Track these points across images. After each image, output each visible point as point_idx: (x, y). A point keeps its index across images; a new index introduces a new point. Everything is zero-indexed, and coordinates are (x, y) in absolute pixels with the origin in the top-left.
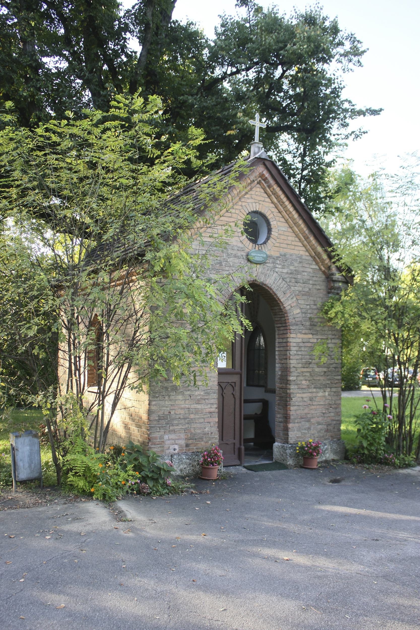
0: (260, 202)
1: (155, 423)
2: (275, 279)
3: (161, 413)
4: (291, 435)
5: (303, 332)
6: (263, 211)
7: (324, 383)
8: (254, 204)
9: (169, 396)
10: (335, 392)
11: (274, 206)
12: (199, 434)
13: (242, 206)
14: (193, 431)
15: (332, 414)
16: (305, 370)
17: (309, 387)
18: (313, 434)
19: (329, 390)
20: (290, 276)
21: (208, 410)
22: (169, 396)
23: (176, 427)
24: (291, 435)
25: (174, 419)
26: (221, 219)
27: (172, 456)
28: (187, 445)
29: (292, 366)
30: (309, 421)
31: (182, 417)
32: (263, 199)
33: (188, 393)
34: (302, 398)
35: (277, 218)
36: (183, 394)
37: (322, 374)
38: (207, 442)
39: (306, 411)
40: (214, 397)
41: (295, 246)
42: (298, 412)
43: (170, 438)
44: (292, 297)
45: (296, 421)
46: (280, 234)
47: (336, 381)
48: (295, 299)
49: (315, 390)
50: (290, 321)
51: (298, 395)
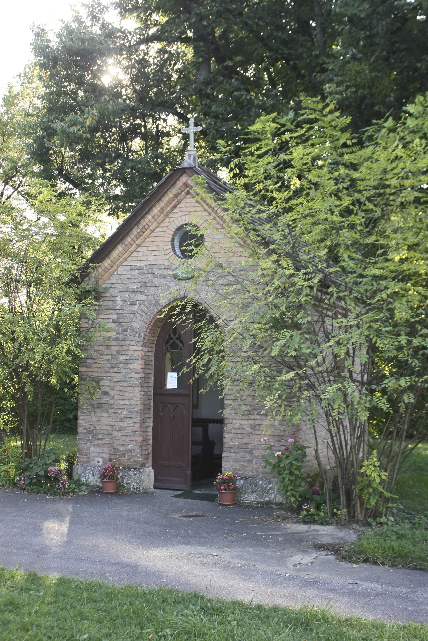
0: (191, 213)
3: (87, 427)
4: (226, 465)
8: (184, 217)
9: (95, 412)
12: (122, 450)
13: (170, 222)
14: (116, 447)
17: (249, 413)
18: (256, 469)
21: (130, 429)
23: (100, 442)
24: (226, 465)
25: (98, 434)
27: (94, 468)
28: (110, 460)
30: (250, 452)
31: (106, 433)
32: (193, 209)
33: (112, 410)
36: (108, 412)
38: (130, 459)
39: (246, 440)
42: (236, 441)
45: (232, 451)
49: (258, 417)
51: (234, 421)
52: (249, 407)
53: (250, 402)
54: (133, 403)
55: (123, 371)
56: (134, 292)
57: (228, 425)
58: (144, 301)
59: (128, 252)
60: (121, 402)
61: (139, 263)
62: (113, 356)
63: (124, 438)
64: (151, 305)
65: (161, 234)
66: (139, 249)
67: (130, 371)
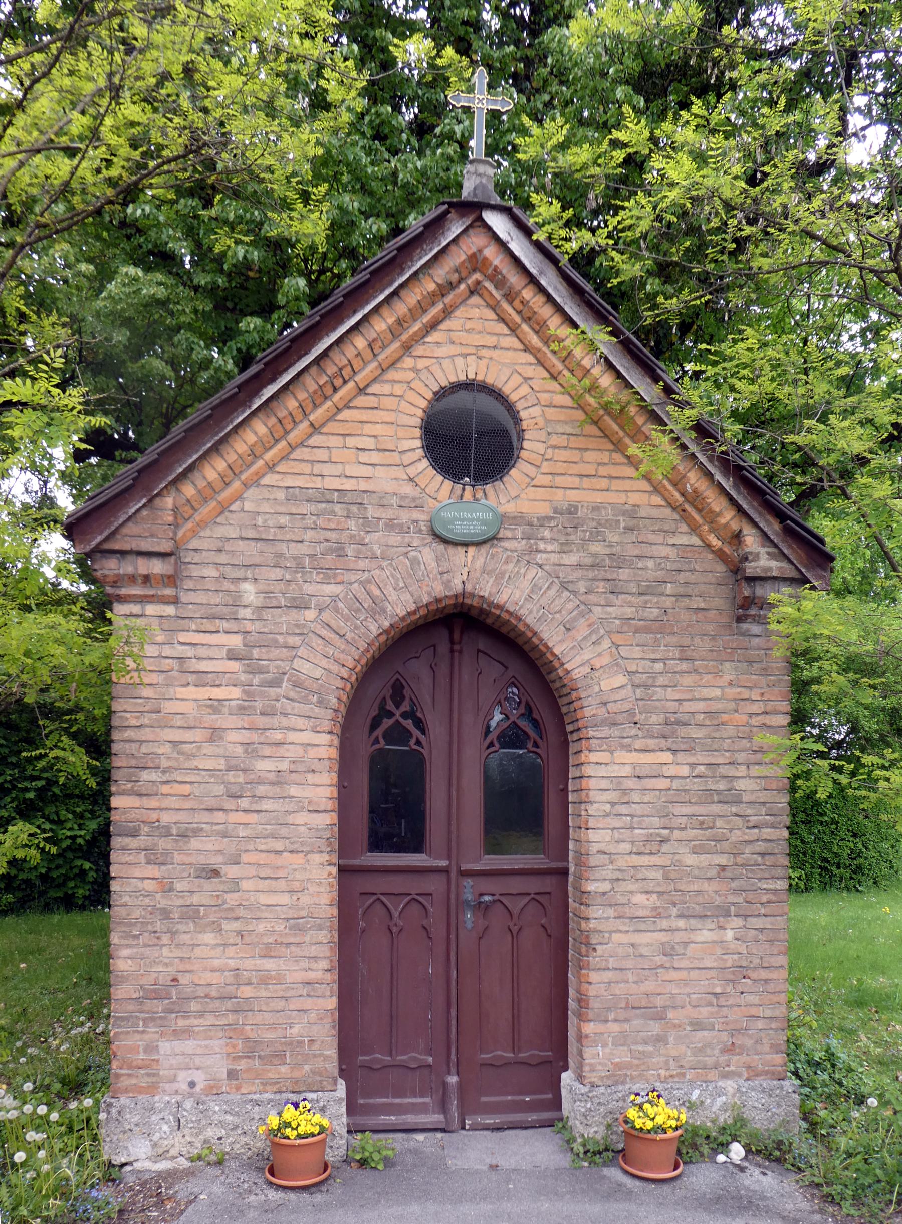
0: (484, 352)
1: (131, 1008)
2: (535, 588)
5: (638, 744)
6: (490, 380)
7: (718, 900)
8: (460, 361)
9: (173, 933)
10: (761, 930)
11: (531, 359)
12: (269, 1043)
14: (252, 1035)
15: (753, 999)
16: (645, 860)
17: (658, 914)
19: (738, 922)
20: (591, 574)
21: (300, 976)
22: (173, 933)
23: (196, 1022)
26: (339, 417)
29: (594, 848)
30: (660, 1017)
31: (214, 994)
32: (491, 341)
33: (236, 925)
34: (633, 945)
35: (544, 397)
37: (713, 873)
39: (649, 986)
40: (320, 939)
41: (611, 478)
42: (618, 990)
43: (177, 1050)
44: (594, 638)
45: (612, 1016)
46: (555, 447)
47: (764, 899)
48: (606, 644)
49: (681, 923)
50: (588, 712)
51: (615, 936)
52: (655, 896)
53: (659, 884)
54: (305, 899)
55: (267, 805)
56: (300, 567)
57: (598, 947)
58: (335, 598)
59: (283, 443)
60: (264, 899)
61: (318, 483)
62: (233, 762)
63: (281, 1004)
64: (357, 611)
65: (387, 402)
66: (316, 440)
67: (292, 807)
